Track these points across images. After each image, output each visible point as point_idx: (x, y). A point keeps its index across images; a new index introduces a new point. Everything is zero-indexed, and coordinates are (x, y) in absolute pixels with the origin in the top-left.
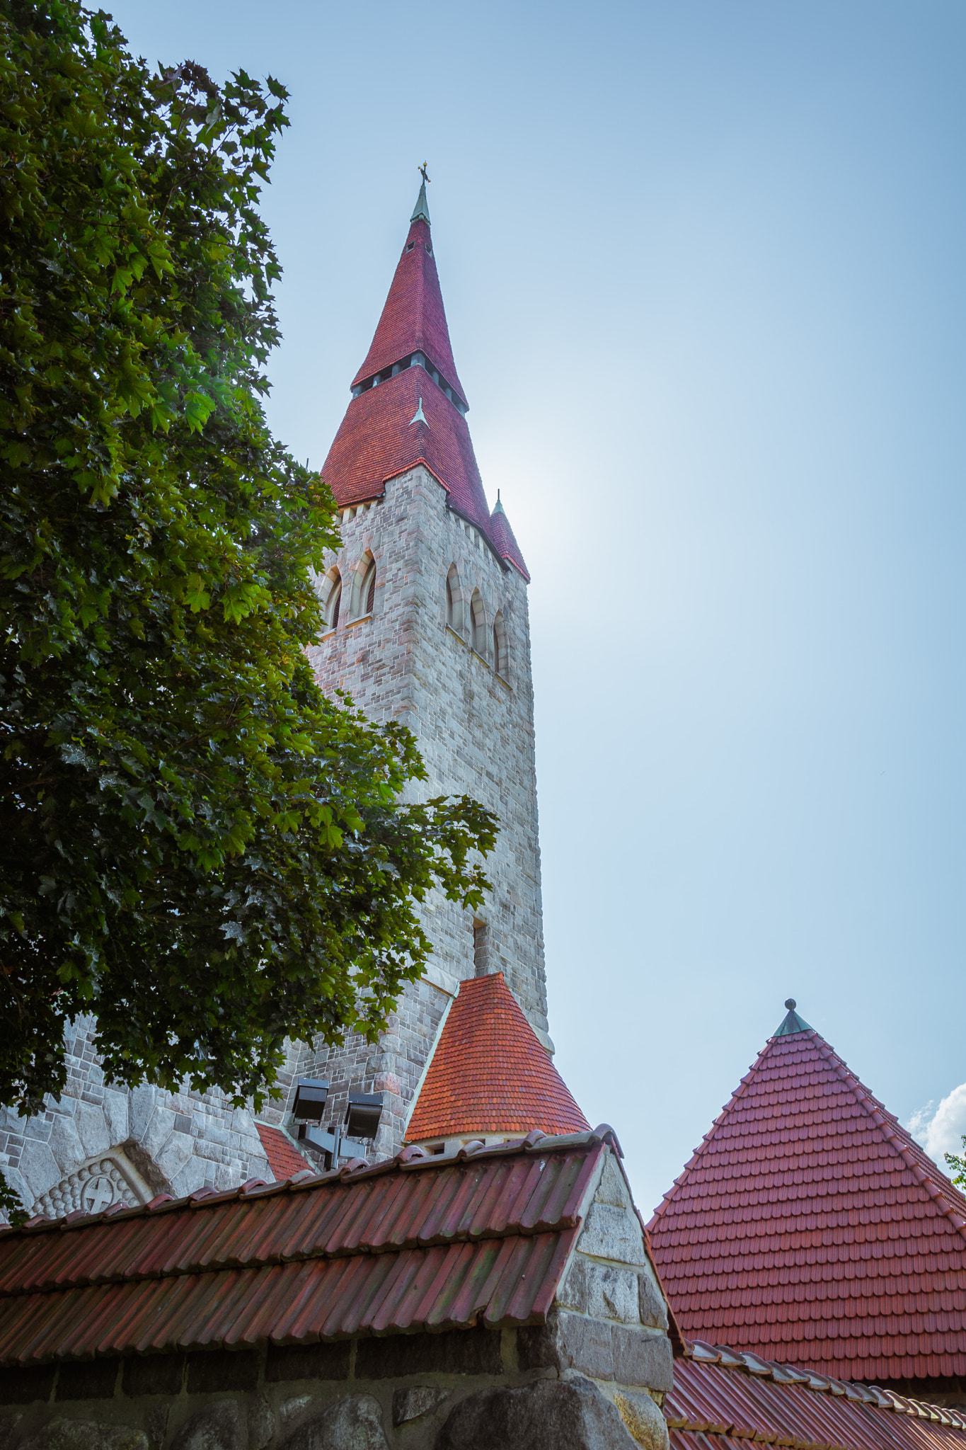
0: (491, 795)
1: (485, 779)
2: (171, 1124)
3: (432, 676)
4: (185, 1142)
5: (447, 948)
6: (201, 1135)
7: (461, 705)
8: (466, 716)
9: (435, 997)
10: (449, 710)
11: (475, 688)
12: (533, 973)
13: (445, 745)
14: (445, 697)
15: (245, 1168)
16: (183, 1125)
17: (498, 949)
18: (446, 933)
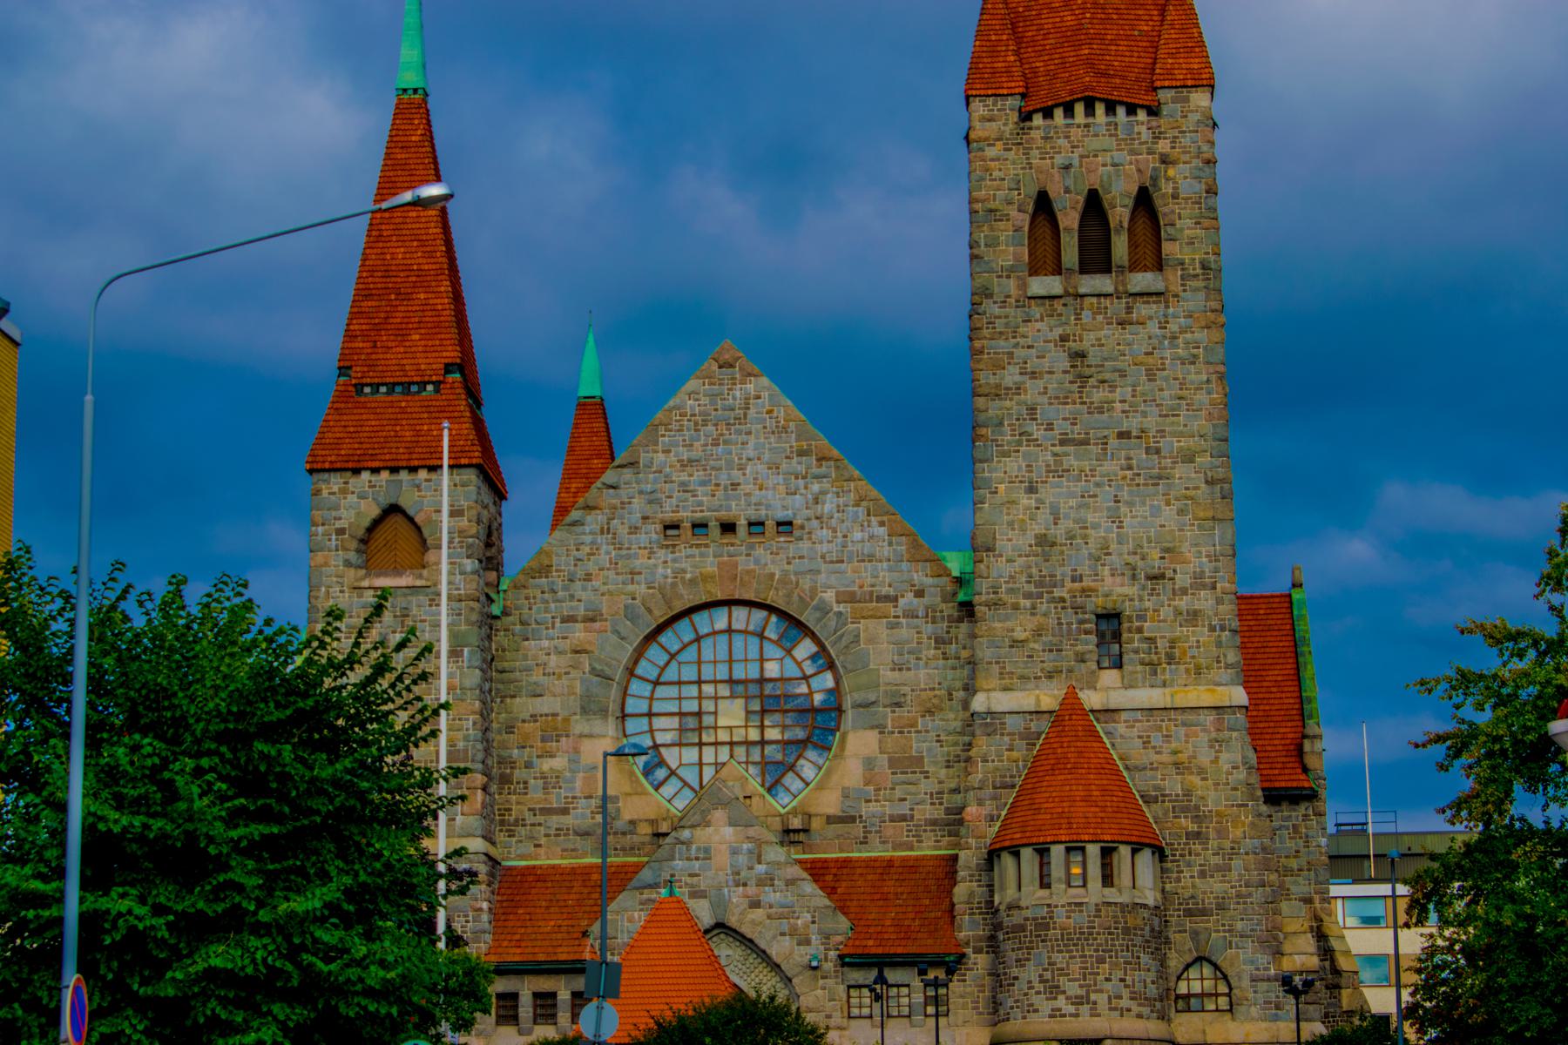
0: (1129, 458)
1: (1113, 442)
2: (745, 905)
3: (1011, 376)
4: (759, 914)
5: (1048, 666)
6: (771, 907)
7: (1069, 377)
8: (1075, 387)
9: (1031, 720)
10: (1045, 399)
11: (1087, 342)
12: (1212, 629)
13: (1038, 445)
15: (813, 917)
16: (755, 904)
17: (1140, 630)
18: (1051, 651)
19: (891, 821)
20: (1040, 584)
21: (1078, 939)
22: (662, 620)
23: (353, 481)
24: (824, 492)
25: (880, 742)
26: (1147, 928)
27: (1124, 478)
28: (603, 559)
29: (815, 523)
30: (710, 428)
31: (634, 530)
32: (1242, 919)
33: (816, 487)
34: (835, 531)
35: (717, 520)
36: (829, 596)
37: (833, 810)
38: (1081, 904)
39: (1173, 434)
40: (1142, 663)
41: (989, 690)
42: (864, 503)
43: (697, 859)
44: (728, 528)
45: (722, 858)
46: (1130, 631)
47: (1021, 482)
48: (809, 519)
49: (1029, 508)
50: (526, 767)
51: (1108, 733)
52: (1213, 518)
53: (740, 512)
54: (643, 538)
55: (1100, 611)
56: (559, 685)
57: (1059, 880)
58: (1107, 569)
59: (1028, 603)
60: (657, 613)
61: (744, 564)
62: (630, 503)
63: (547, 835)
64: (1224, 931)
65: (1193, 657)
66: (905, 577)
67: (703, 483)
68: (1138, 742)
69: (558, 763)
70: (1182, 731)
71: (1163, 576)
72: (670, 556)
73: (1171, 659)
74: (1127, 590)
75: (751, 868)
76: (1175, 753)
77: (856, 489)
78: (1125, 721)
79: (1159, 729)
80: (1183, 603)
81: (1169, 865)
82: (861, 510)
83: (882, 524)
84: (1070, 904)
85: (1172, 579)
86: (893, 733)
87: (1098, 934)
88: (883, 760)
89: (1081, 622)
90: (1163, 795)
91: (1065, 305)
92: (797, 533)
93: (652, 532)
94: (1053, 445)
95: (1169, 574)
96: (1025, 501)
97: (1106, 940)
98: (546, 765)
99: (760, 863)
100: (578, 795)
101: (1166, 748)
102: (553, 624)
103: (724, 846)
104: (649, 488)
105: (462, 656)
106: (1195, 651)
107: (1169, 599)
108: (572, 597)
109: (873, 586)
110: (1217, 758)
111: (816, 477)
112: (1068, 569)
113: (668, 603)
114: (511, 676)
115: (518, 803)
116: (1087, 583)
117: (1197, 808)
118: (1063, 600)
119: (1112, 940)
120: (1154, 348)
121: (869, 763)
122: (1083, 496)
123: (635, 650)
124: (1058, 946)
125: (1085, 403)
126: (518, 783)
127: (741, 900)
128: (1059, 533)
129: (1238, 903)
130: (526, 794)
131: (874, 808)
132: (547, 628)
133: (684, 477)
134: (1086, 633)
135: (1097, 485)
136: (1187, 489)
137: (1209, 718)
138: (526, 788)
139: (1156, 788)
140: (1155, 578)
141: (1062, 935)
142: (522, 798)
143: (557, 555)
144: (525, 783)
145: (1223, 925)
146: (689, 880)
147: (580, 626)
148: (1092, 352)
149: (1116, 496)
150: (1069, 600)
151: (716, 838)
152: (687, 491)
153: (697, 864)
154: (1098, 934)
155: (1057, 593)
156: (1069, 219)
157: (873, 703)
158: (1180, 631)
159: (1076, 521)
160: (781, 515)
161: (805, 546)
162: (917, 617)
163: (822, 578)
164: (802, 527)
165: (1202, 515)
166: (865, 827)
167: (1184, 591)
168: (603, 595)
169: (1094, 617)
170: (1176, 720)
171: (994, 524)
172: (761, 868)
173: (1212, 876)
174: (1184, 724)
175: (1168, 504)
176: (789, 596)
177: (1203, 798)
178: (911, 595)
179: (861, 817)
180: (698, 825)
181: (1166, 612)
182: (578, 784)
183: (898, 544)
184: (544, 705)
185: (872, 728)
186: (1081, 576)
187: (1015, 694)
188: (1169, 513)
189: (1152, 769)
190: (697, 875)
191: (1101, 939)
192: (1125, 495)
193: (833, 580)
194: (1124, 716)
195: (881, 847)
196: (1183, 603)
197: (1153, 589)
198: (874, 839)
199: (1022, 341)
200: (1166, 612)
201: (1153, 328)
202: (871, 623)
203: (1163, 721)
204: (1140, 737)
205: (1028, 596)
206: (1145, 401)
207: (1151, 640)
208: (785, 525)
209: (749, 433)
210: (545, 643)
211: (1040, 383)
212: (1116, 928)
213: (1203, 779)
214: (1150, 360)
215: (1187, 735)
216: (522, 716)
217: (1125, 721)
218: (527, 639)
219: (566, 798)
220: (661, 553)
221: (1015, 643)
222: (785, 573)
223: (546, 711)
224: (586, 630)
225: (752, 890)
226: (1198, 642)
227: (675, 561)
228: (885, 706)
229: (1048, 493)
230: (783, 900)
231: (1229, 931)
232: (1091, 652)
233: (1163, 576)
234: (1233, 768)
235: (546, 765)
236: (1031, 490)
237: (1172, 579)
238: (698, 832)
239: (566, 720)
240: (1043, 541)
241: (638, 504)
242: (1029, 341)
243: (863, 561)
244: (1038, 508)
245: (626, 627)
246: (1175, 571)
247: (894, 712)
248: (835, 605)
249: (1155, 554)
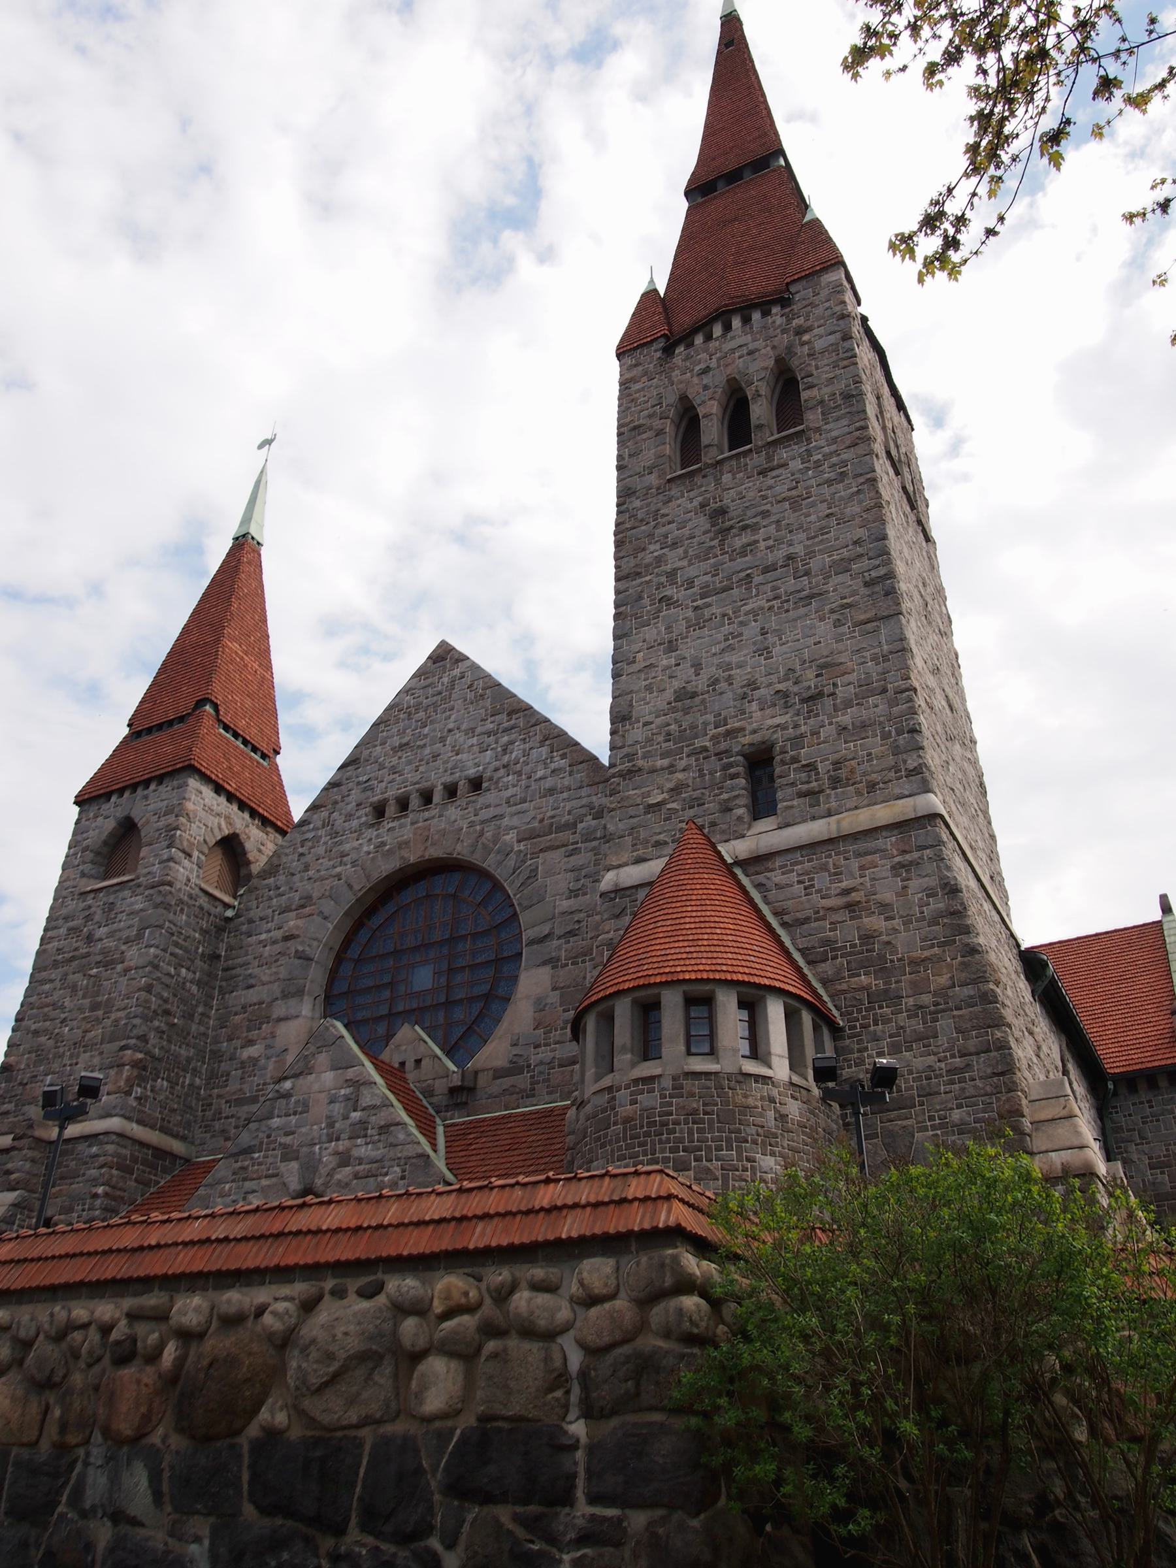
10: (685, 563)
14: (674, 559)
15: (404, 1171)
16: (344, 1159)
18: (691, 807)
19: (561, 1066)
20: (681, 739)
21: (647, 1134)
22: (360, 894)
23: (105, 806)
24: (512, 743)
25: (553, 977)
26: (771, 1114)
27: (770, 608)
28: (321, 850)
29: (502, 772)
30: (422, 714)
31: (349, 817)
32: (959, 1106)
33: (505, 739)
34: (519, 773)
35: (417, 791)
36: (511, 837)
37: (501, 1062)
38: (652, 1079)
39: (822, 552)
40: (801, 795)
41: (619, 866)
42: (547, 743)
43: (295, 1113)
44: (427, 798)
45: (320, 1109)
46: (783, 763)
47: (660, 644)
48: (496, 770)
49: (668, 667)
50: (230, 1060)
51: (759, 886)
52: (876, 619)
53: (437, 779)
54: (355, 823)
55: (747, 750)
56: (265, 974)
57: (624, 1049)
58: (754, 706)
59: (665, 762)
60: (357, 887)
61: (438, 824)
62: (348, 795)
63: (236, 1127)
64: (934, 1128)
65: (865, 774)
66: (584, 801)
67: (409, 763)
68: (798, 889)
69: (253, 1051)
70: (855, 864)
71: (820, 694)
72: (375, 833)
73: (835, 782)
74: (778, 720)
75: (346, 1117)
76: (846, 892)
77: (540, 730)
78: (781, 867)
79: (824, 868)
80: (845, 719)
81: (847, 1042)
82: (544, 750)
83: (563, 756)
84: (636, 1081)
85: (833, 694)
86: (567, 965)
87: (677, 1123)
88: (554, 997)
89: (726, 768)
90: (833, 950)
91: (704, 477)
92: (485, 785)
93: (365, 815)
94: (693, 601)
95: (828, 689)
96: (665, 662)
97: (690, 1132)
98: (247, 1053)
99: (355, 1111)
100: (268, 1081)
101: (836, 887)
102: (273, 917)
103: (323, 1095)
104: (365, 778)
105: (143, 938)
106: (866, 766)
107: (830, 716)
108: (291, 888)
109: (553, 817)
110: (905, 887)
111: (505, 730)
112: (710, 718)
113: (368, 877)
114: (234, 972)
115: (219, 1096)
116: (734, 724)
117: (882, 957)
118: (705, 749)
119: (700, 1131)
120: (797, 483)
121: (540, 1005)
122: (726, 640)
123: (335, 928)
124: (620, 1149)
125: (727, 553)
126: (222, 1076)
127: (331, 1158)
128: (701, 683)
129: (952, 1082)
130: (227, 1086)
131: (544, 1054)
132: (267, 923)
133: (395, 761)
134: (734, 777)
135: (742, 624)
136: (842, 598)
137: (889, 842)
138: (227, 1080)
139: (826, 942)
140: (811, 698)
141: (625, 1130)
142: (223, 1091)
143: (287, 855)
144: (228, 1074)
145: (931, 1118)
146: (283, 1140)
147: (293, 914)
148: (732, 506)
149: (762, 629)
150: (711, 749)
151: (316, 1087)
152: (395, 773)
153: (293, 1119)
154: (677, 1123)
155: (698, 743)
156: (711, 411)
157: (546, 937)
158: (846, 749)
159: (719, 666)
160: (472, 772)
161: (491, 797)
162: (595, 839)
163: (506, 822)
164: (491, 779)
165: (862, 617)
166: (532, 1077)
167: (848, 704)
168: (315, 882)
169: (740, 758)
170: (846, 852)
171: (631, 692)
172: (356, 1115)
173: (909, 1049)
174: (859, 855)
175: (822, 619)
176: (474, 846)
177: (889, 943)
178: (589, 818)
179: (529, 1066)
180: (301, 1074)
181: (828, 731)
182: (271, 1067)
183: (578, 772)
184: (252, 996)
185: (544, 963)
186: (725, 719)
187: (650, 863)
188: (824, 628)
189: (817, 920)
190: (293, 1133)
191: (682, 1131)
192: (773, 623)
193: (515, 821)
194: (778, 862)
195: (547, 1098)
196: (845, 719)
197: (812, 711)
198: (541, 1088)
199: (665, 520)
200: (828, 731)
201: (796, 465)
202: (550, 855)
203: (830, 856)
204: (799, 882)
205: (664, 755)
206: (790, 532)
207: (811, 767)
208: (476, 784)
209: (452, 709)
210: (263, 937)
211: (680, 551)
212: (705, 1113)
213: (887, 919)
214: (794, 493)
215: (862, 868)
216: (234, 1009)
217: (781, 867)
218: (251, 936)
219: (258, 1085)
220: (371, 833)
221: (651, 808)
222: (472, 824)
223: (255, 1000)
224: (298, 917)
225: (342, 1145)
226: (869, 754)
227: (378, 836)
228: (559, 938)
229: (688, 649)
230: (374, 1154)
231: (941, 1126)
232: (737, 797)
233: (820, 694)
234: (928, 896)
235: (247, 1053)
236: (671, 647)
237: (833, 694)
238: (301, 1081)
239: (270, 1005)
240: (684, 696)
241: (355, 795)
242: (669, 518)
243: (545, 796)
244: (678, 665)
245: (328, 906)
246: (834, 685)
247: (569, 942)
248: (516, 845)
249: (811, 674)
